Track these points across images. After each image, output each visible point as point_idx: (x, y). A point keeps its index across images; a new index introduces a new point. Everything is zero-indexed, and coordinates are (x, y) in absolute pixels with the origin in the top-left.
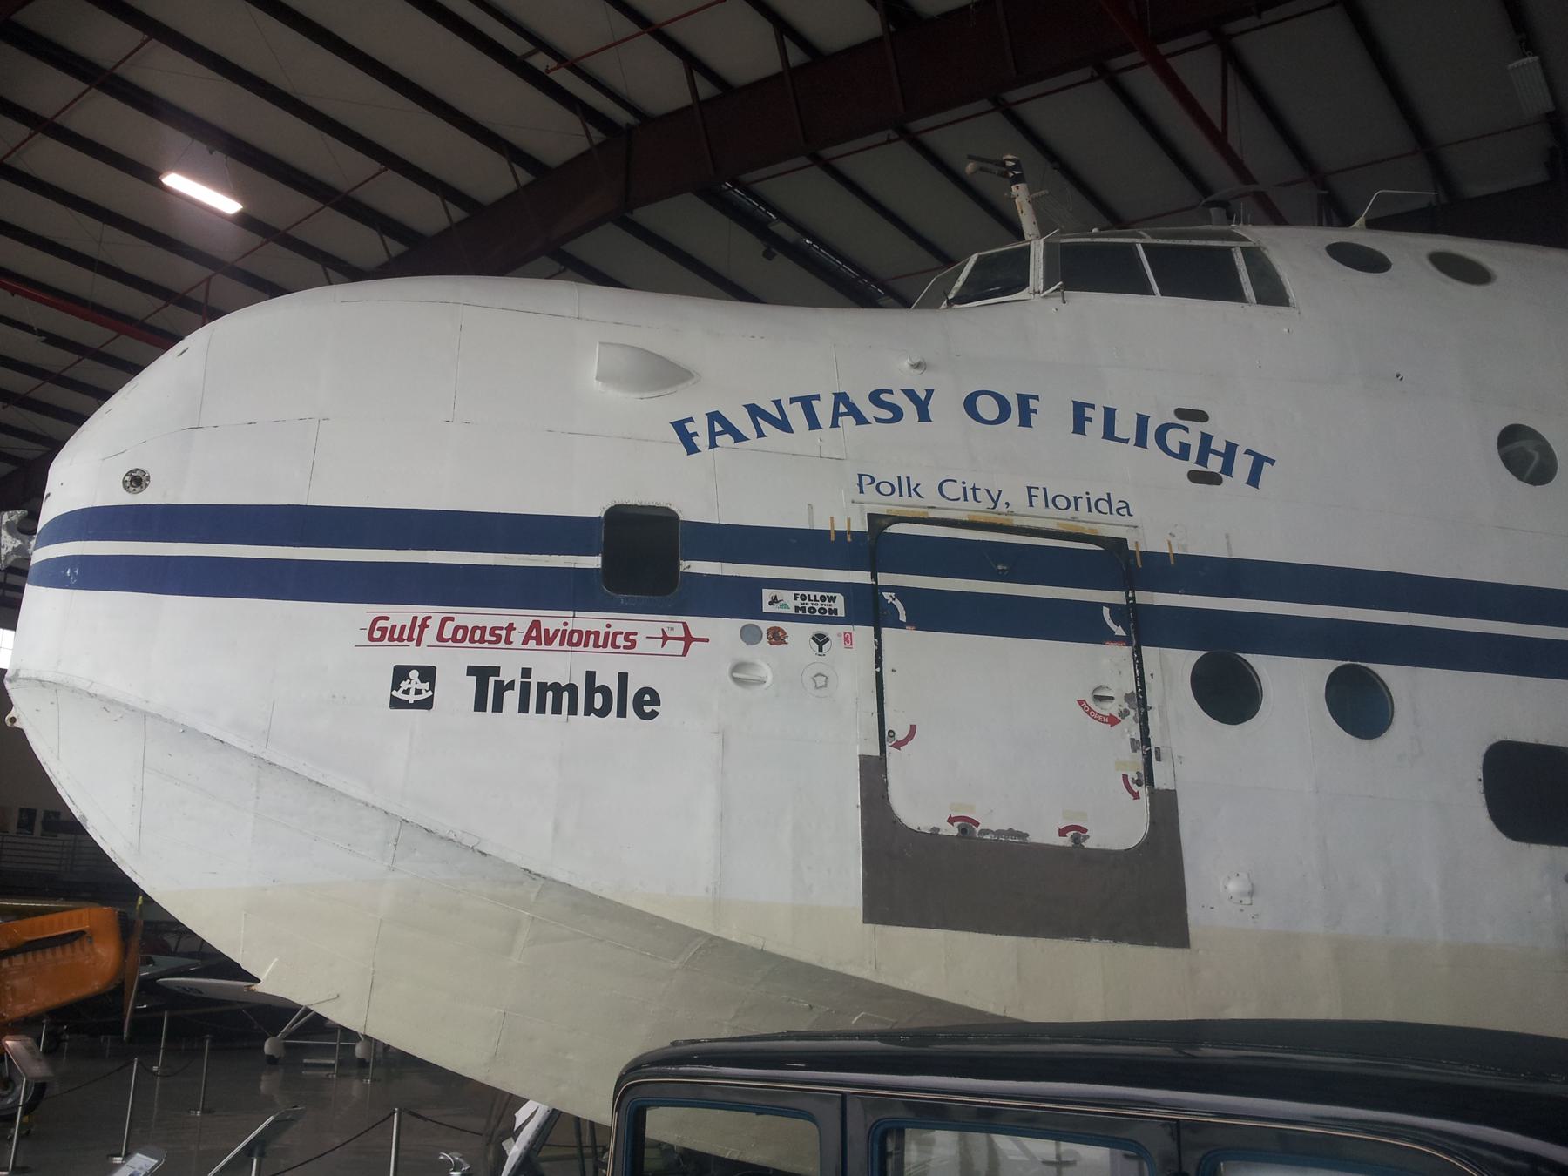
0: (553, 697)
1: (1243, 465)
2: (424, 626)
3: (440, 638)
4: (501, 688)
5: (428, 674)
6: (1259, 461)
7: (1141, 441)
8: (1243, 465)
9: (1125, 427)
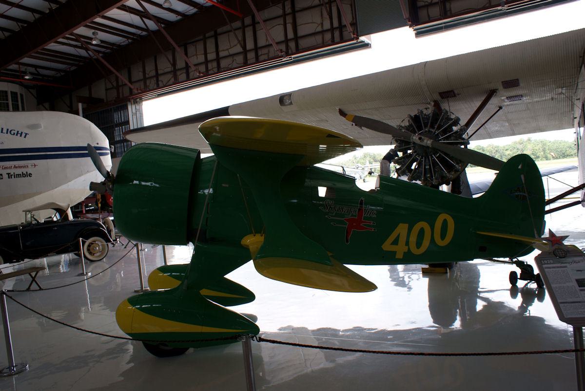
0: (18, 176)
1: (24, 135)
4: (11, 175)
6: (26, 134)
7: (7, 133)
8: (24, 135)
9: (5, 131)
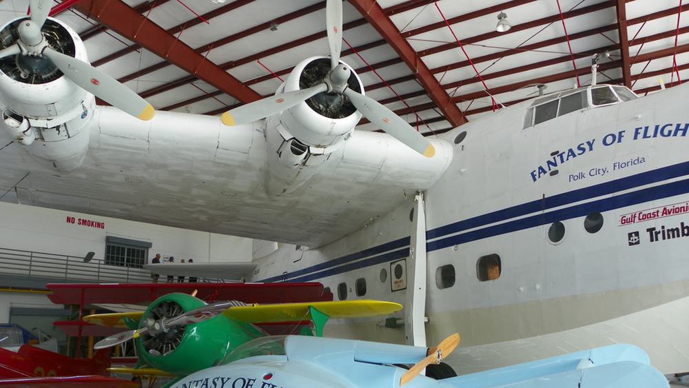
0: (674, 233)
2: (635, 217)
3: (639, 219)
4: (657, 233)
5: (637, 234)
